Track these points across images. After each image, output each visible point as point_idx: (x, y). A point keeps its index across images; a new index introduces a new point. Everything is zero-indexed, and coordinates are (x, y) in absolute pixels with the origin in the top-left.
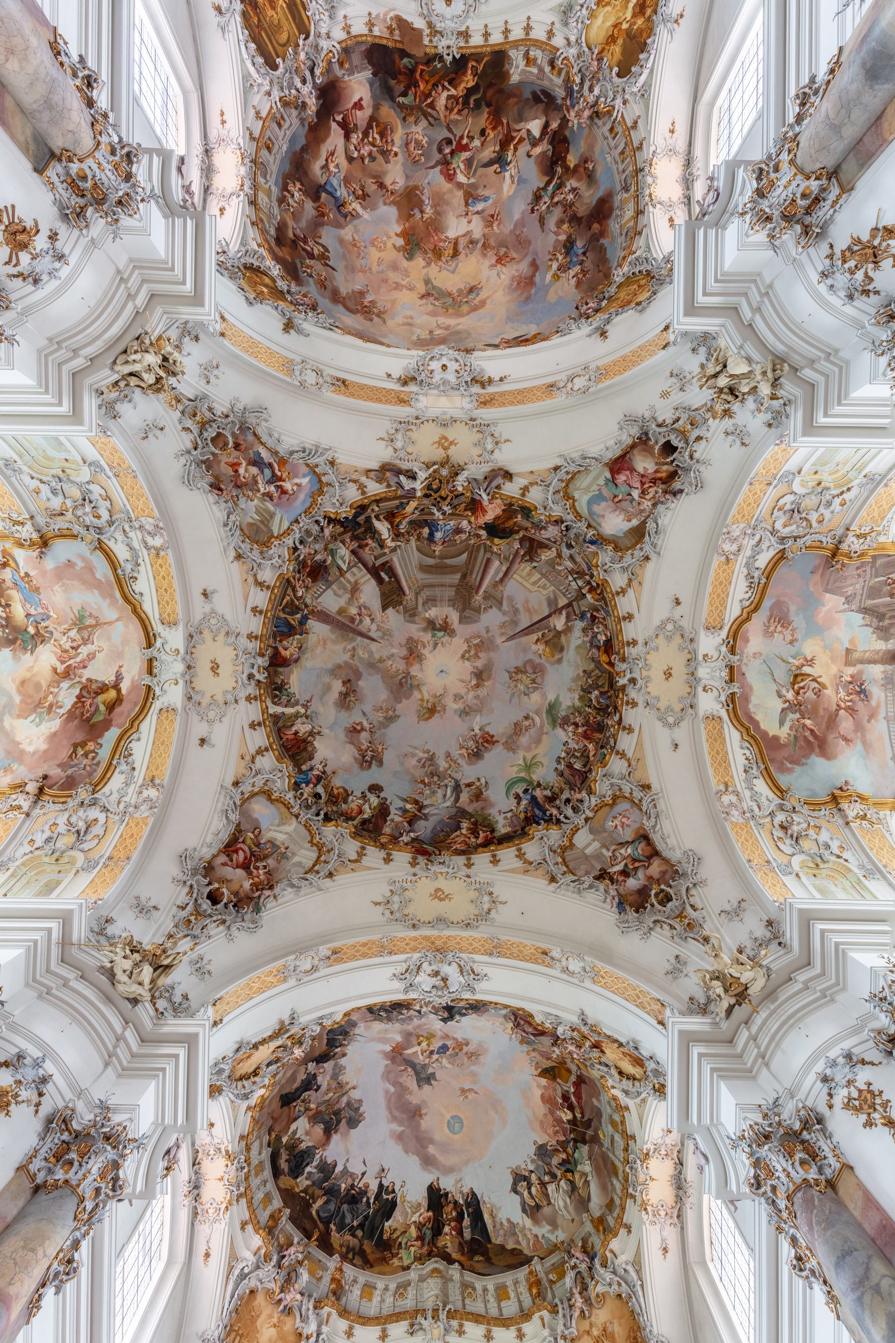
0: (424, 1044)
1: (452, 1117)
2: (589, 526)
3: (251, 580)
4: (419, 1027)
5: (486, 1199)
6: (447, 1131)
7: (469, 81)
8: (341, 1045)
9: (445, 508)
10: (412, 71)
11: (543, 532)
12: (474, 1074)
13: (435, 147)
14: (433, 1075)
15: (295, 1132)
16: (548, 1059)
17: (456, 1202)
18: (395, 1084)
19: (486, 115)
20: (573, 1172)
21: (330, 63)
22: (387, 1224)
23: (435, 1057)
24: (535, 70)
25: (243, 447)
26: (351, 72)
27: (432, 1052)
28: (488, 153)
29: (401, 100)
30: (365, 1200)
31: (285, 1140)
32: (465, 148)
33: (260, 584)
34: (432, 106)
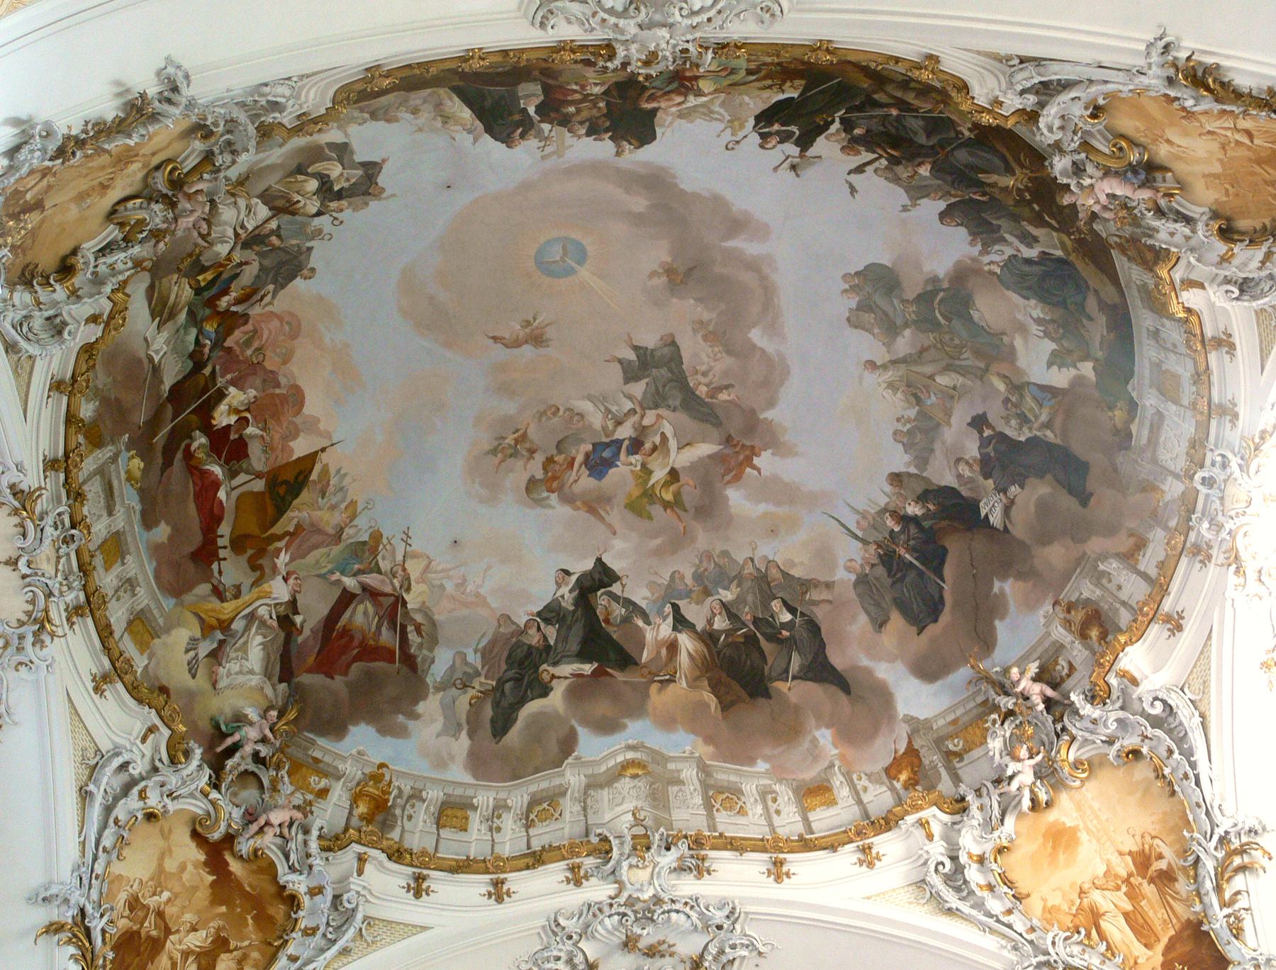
0: (659, 475)
1: (570, 272)
4: (678, 542)
5: (465, 139)
6: (589, 243)
8: (905, 520)
12: (505, 390)
14: (631, 374)
15: (1056, 360)
16: (299, 527)
17: (565, 122)
18: (745, 352)
20: (198, 291)
22: (795, 95)
23: (625, 432)
27: (636, 445)
30: (857, 131)
31: (1087, 369)
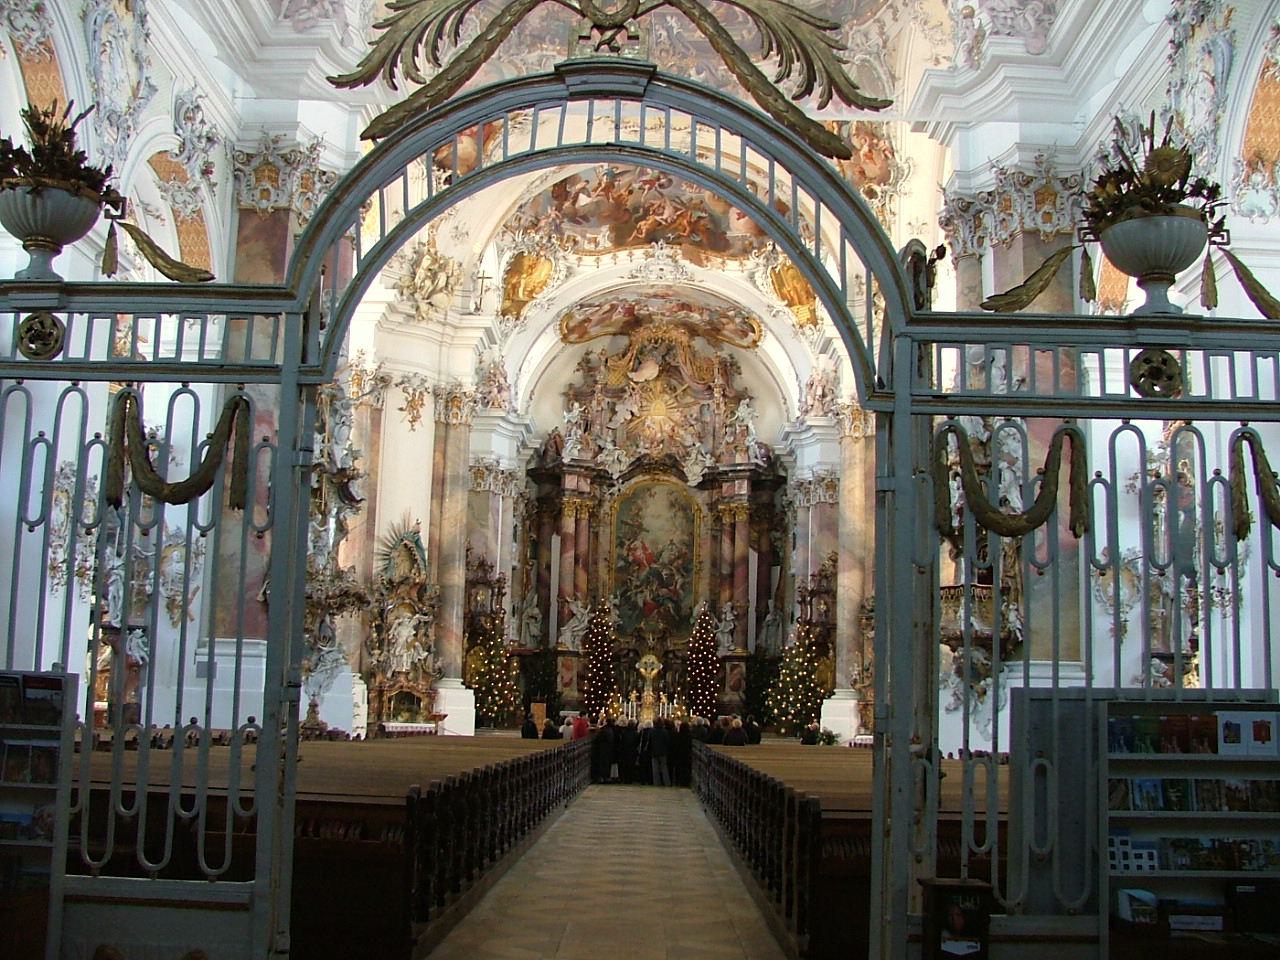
2: (500, 58)
3: (889, 44)
7: (644, 225)
9: (664, 34)
10: (692, 231)
11: (545, 13)
13: (674, 183)
19: (628, 203)
21: (759, 249)
24: (588, 235)
25: (857, 169)
26: (744, 238)
28: (625, 179)
29: (704, 215)
32: (645, 182)
33: (882, 33)
34: (677, 210)
